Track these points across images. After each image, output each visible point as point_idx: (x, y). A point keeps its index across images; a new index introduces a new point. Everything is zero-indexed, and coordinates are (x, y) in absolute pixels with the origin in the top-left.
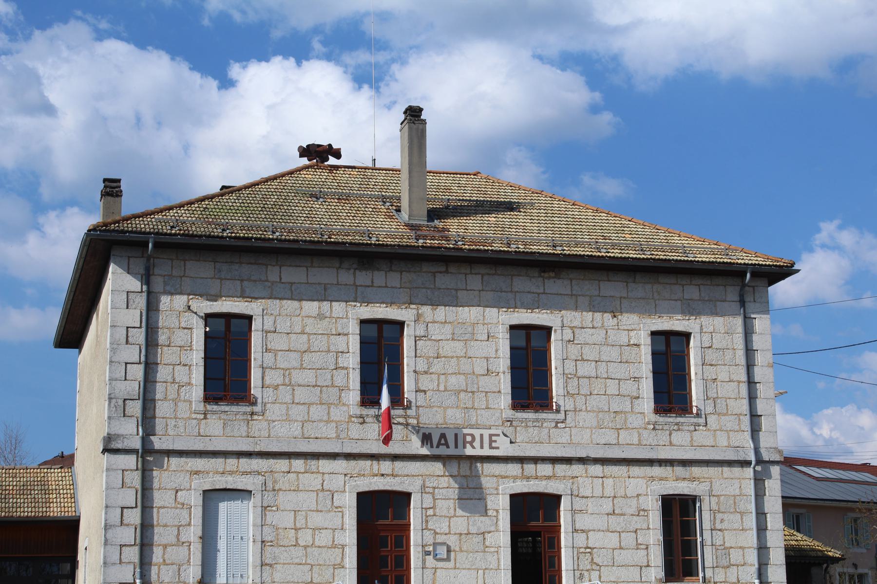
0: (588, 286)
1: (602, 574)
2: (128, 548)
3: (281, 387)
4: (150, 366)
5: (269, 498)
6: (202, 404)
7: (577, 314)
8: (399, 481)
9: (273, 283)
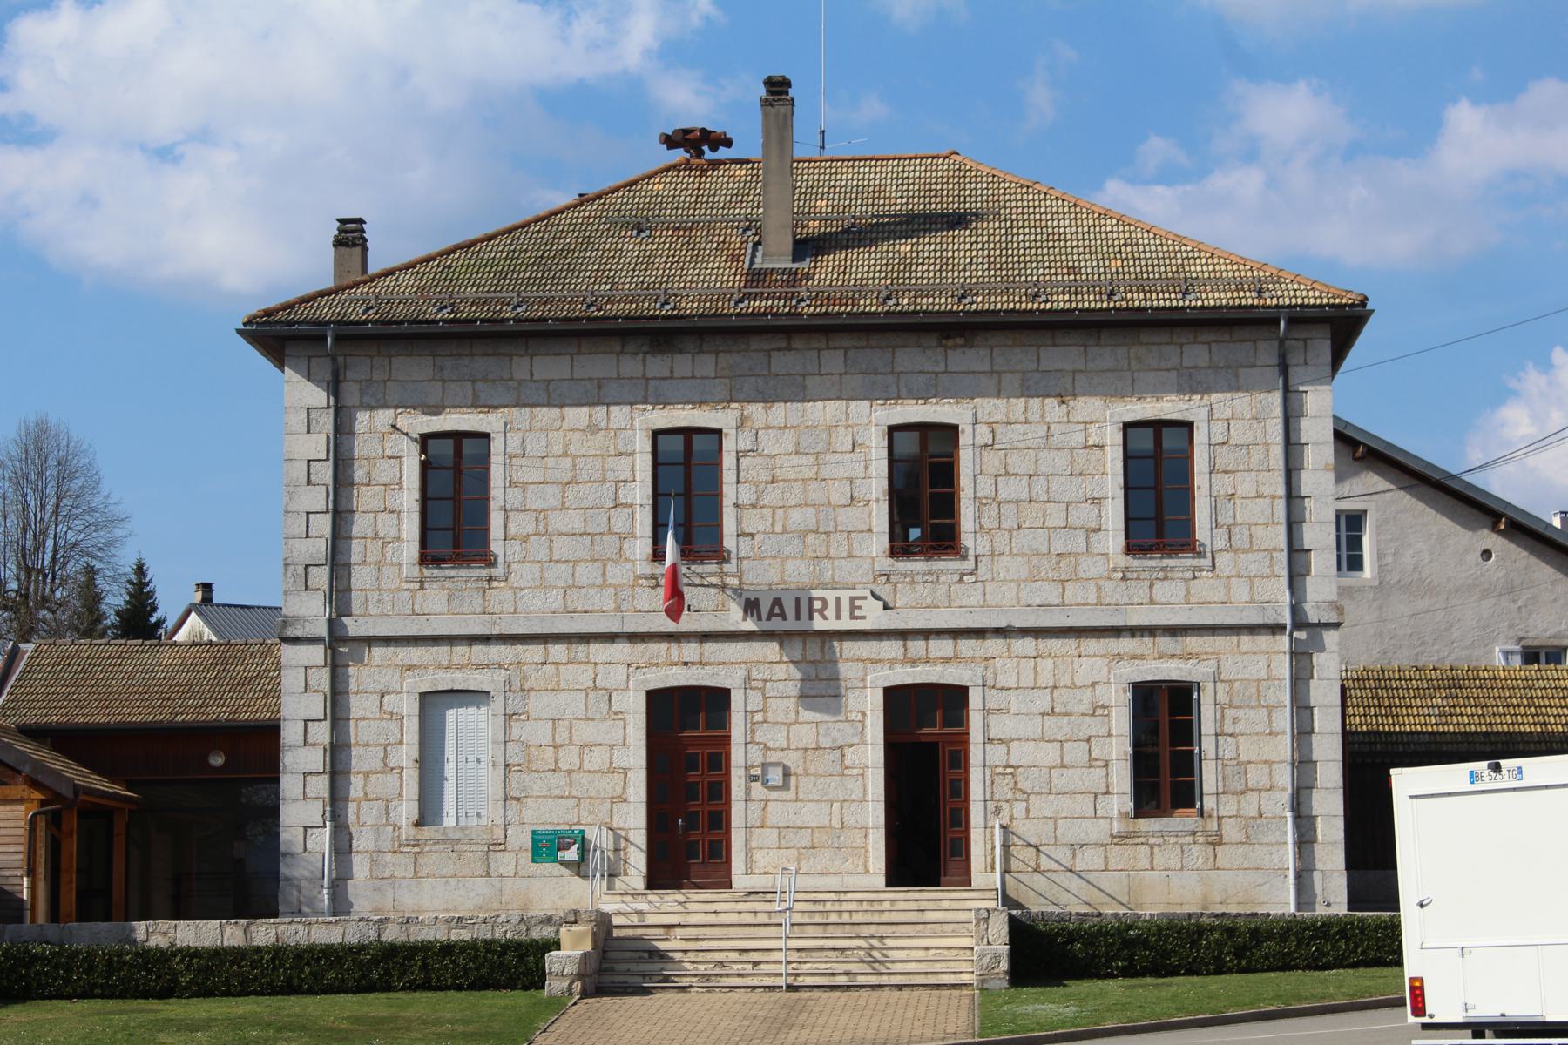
0: (1020, 357)
1: (1031, 807)
2: (315, 778)
3: (532, 538)
4: (341, 515)
5: (515, 702)
6: (417, 567)
7: (1000, 403)
8: (710, 672)
9: (520, 382)
